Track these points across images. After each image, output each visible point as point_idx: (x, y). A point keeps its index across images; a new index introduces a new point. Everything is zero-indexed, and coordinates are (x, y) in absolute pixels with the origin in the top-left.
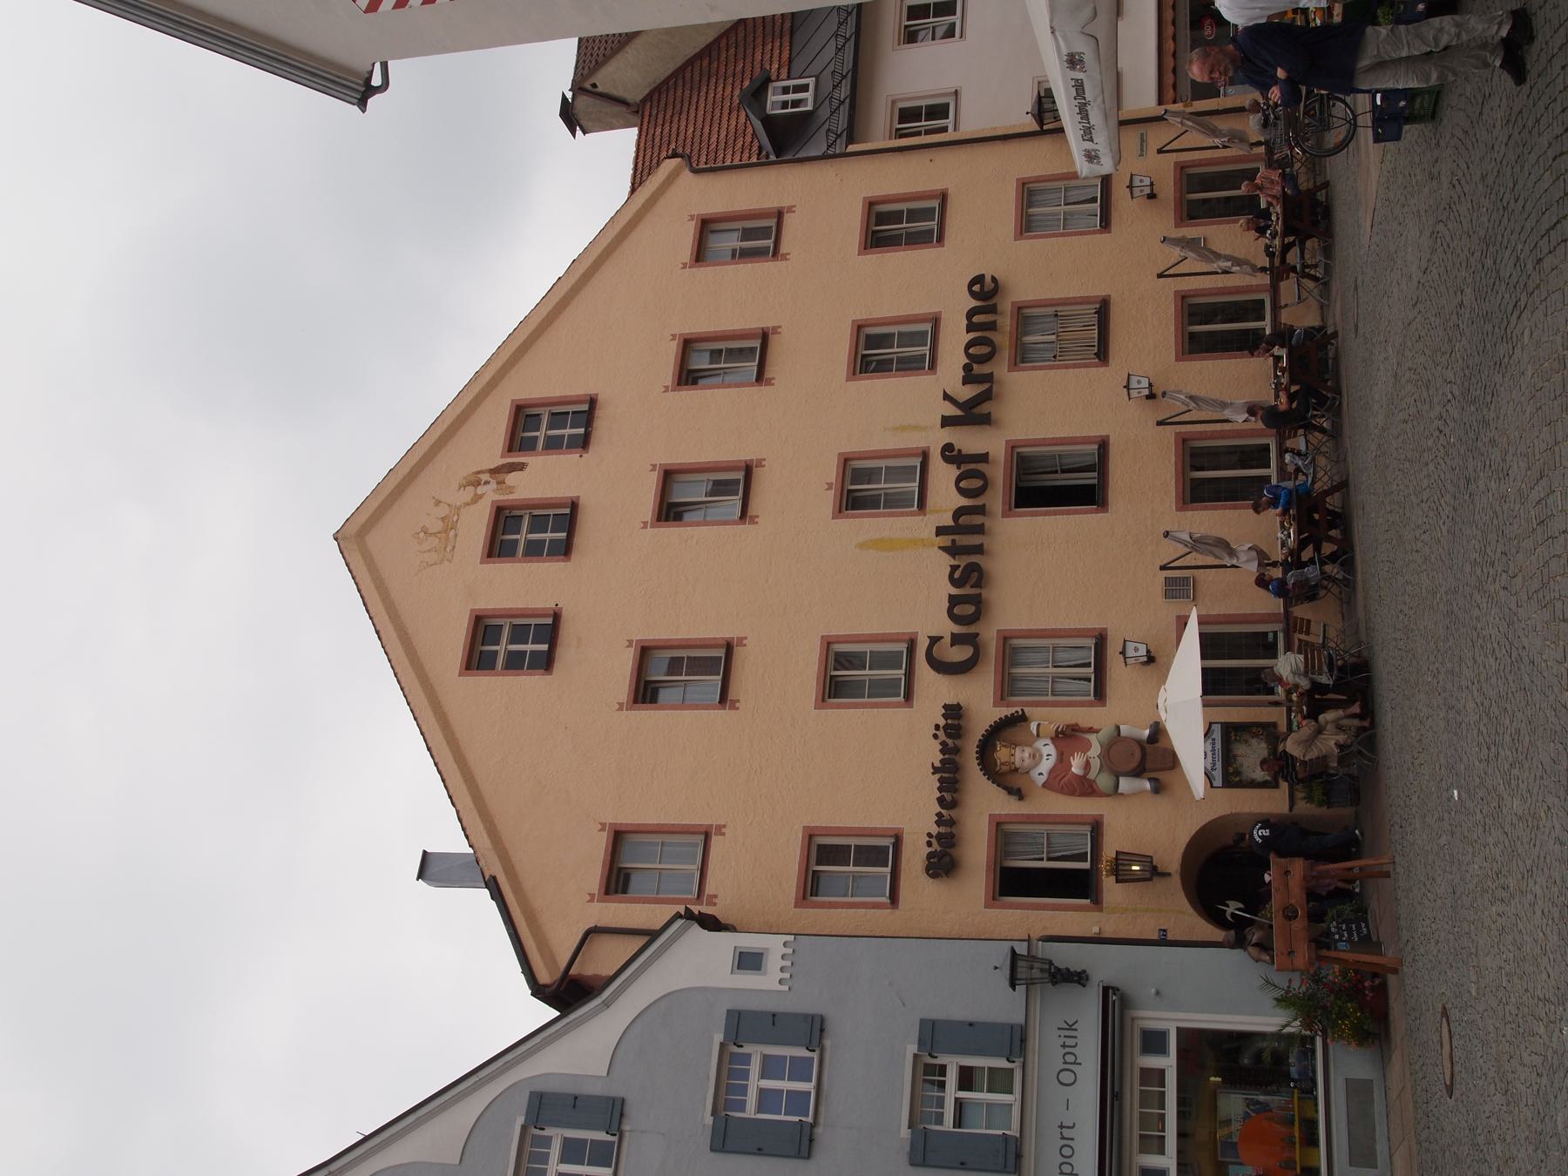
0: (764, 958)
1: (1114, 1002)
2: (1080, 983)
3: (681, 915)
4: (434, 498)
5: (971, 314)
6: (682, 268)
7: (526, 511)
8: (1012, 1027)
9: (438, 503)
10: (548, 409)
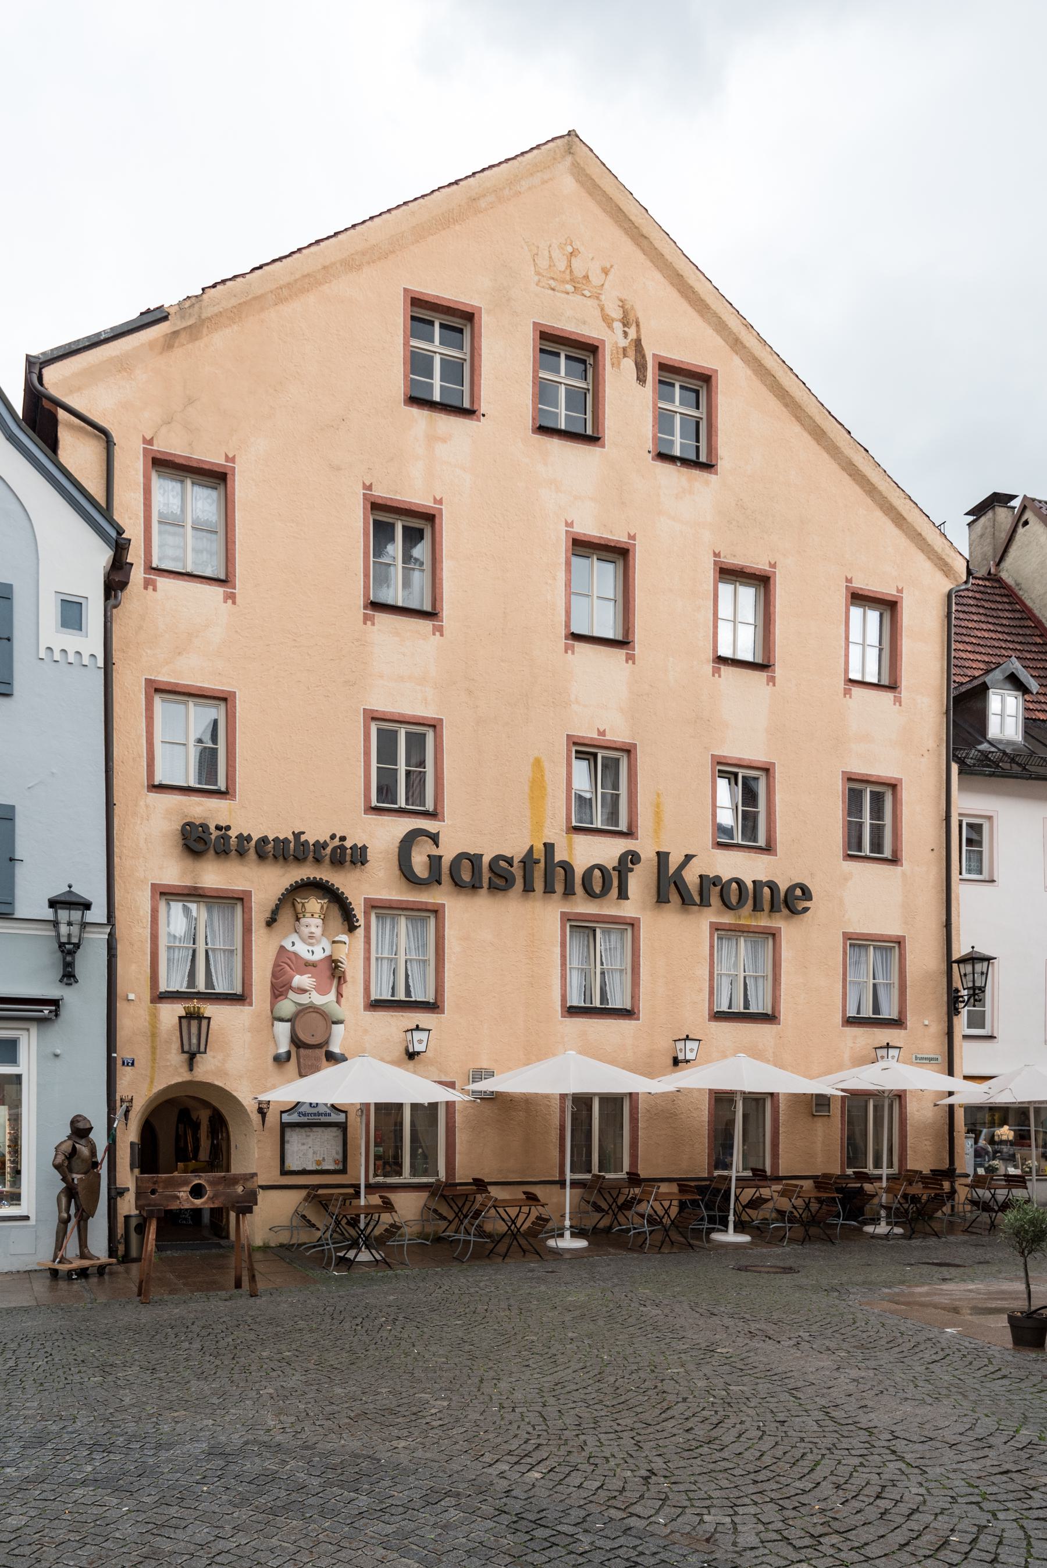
0: (75, 632)
1: (41, 1011)
2: (63, 976)
3: (121, 535)
4: (612, 266)
5: (772, 886)
6: (847, 578)
7: (591, 385)
8: (11, 904)
9: (606, 272)
10: (704, 416)
